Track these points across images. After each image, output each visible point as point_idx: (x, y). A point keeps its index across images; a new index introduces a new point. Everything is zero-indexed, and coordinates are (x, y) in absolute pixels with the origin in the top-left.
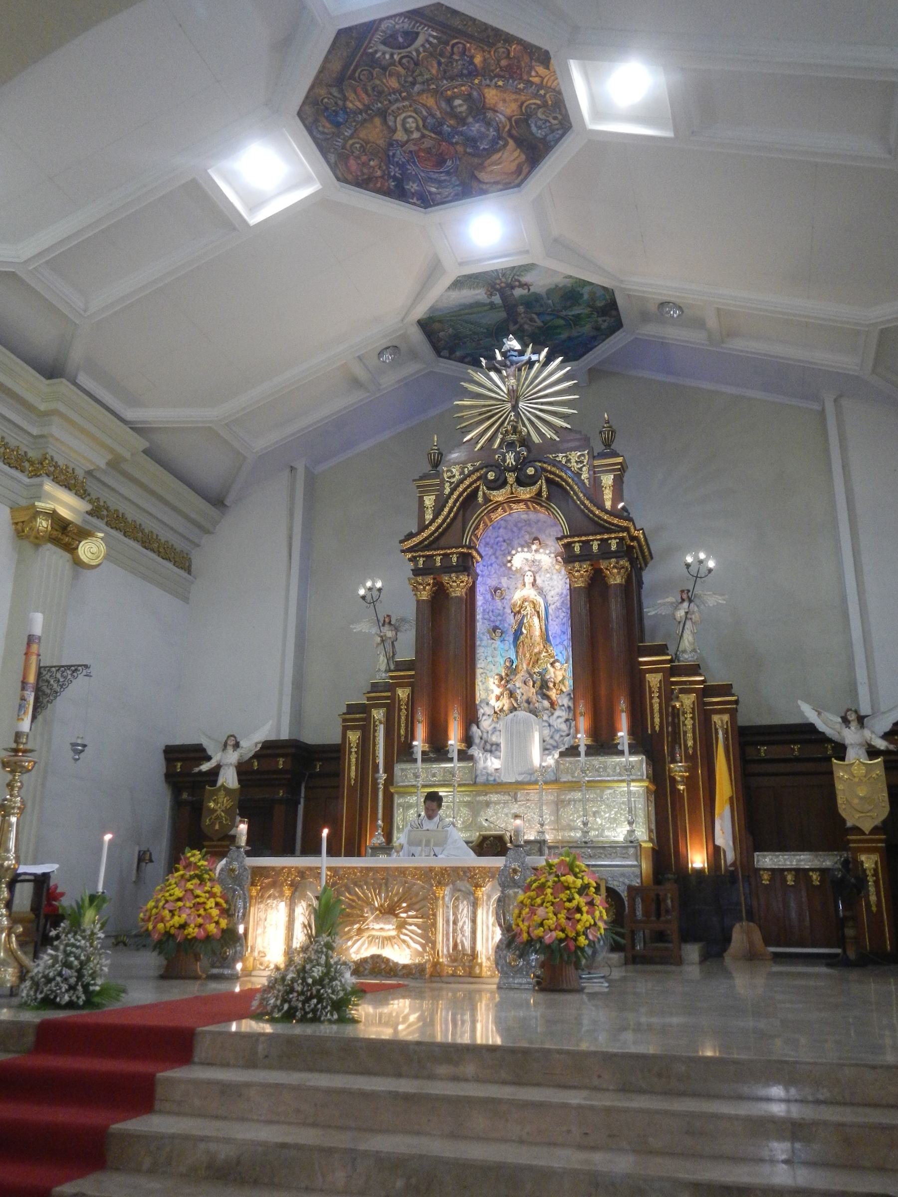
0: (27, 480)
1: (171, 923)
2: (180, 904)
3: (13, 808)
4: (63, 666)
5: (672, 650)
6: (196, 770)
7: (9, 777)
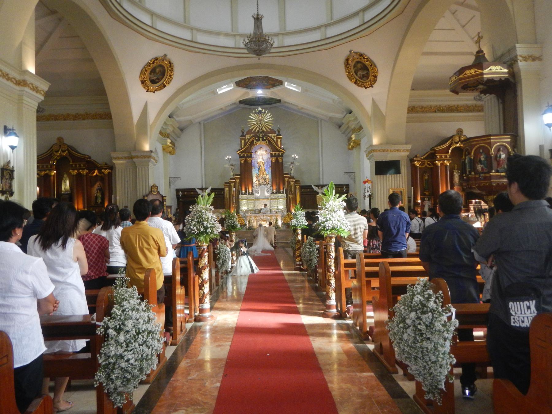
0: (164, 138)
5: (289, 174)
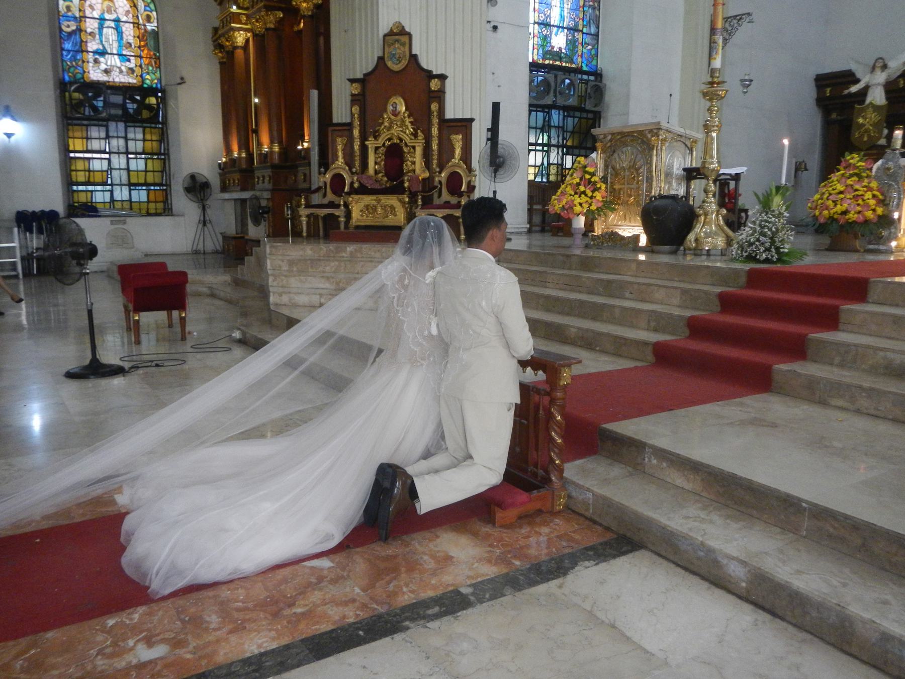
1: (835, 210)
2: (842, 196)
3: (714, 126)
4: (730, 17)
6: (846, 92)
7: (708, 104)
